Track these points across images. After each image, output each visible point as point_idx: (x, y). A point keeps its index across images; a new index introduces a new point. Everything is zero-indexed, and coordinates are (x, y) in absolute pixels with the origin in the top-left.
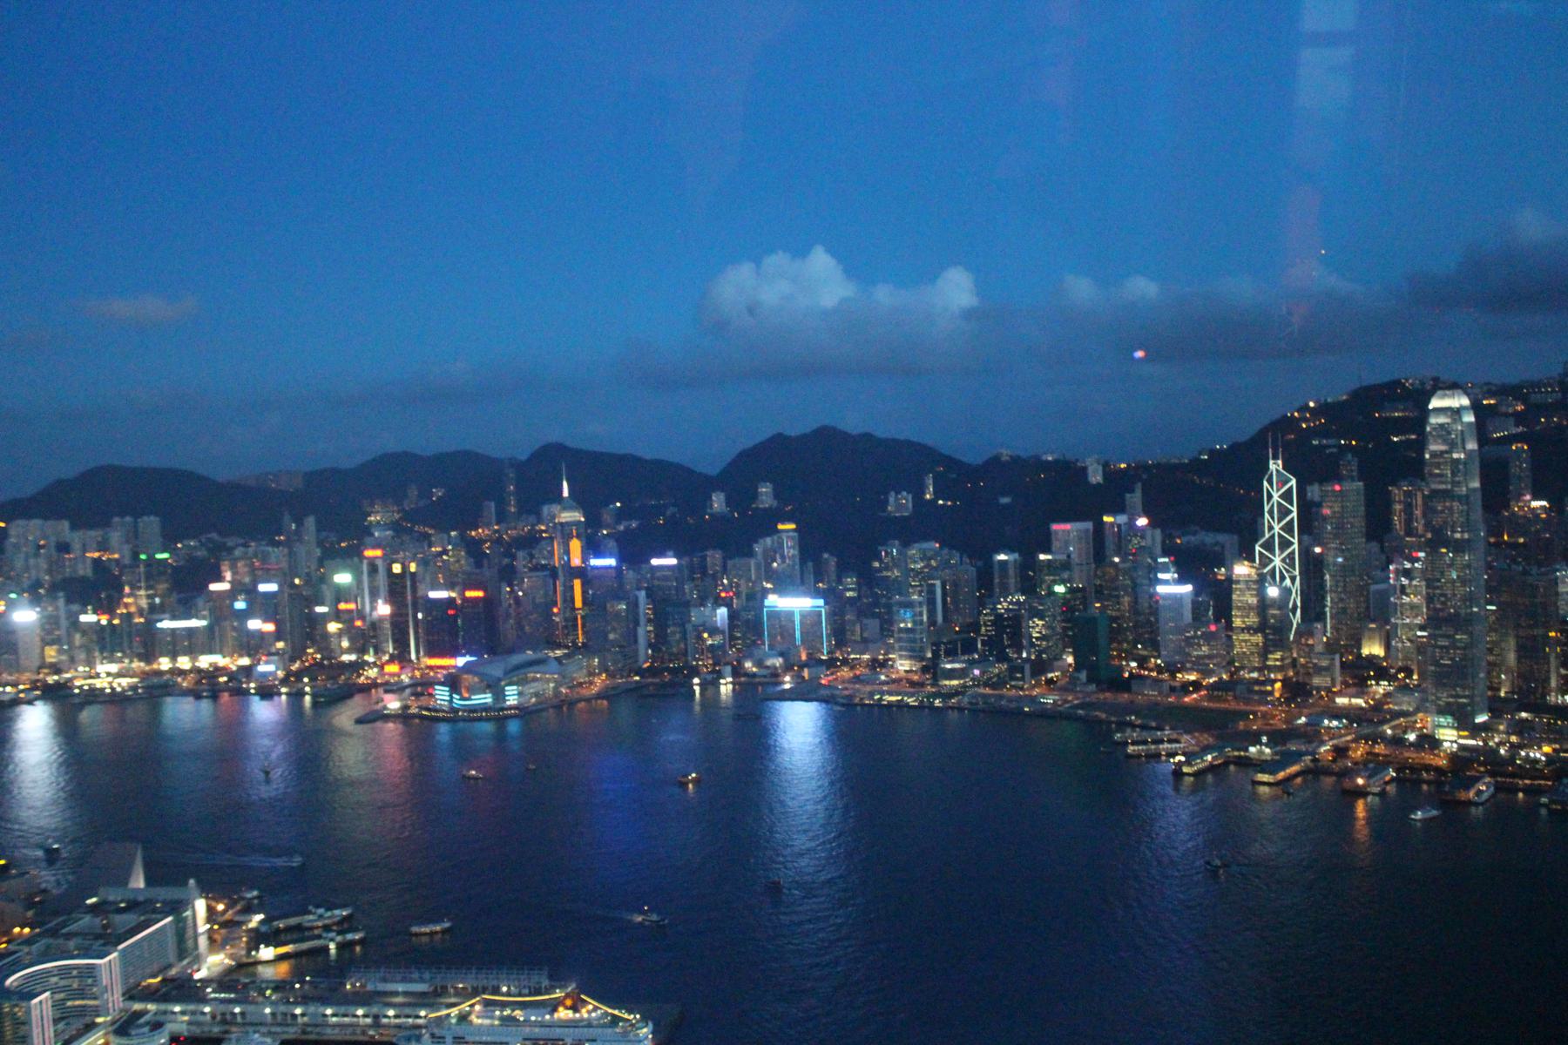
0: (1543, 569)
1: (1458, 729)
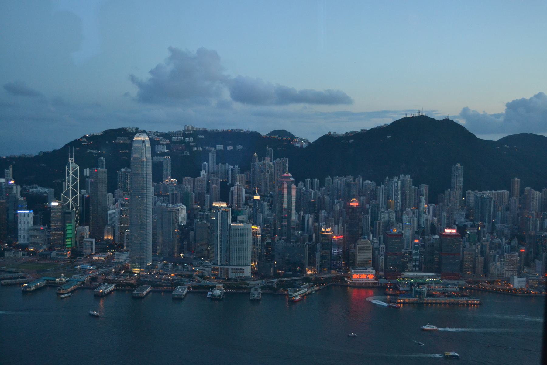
0: (174, 205)
1: (140, 268)
